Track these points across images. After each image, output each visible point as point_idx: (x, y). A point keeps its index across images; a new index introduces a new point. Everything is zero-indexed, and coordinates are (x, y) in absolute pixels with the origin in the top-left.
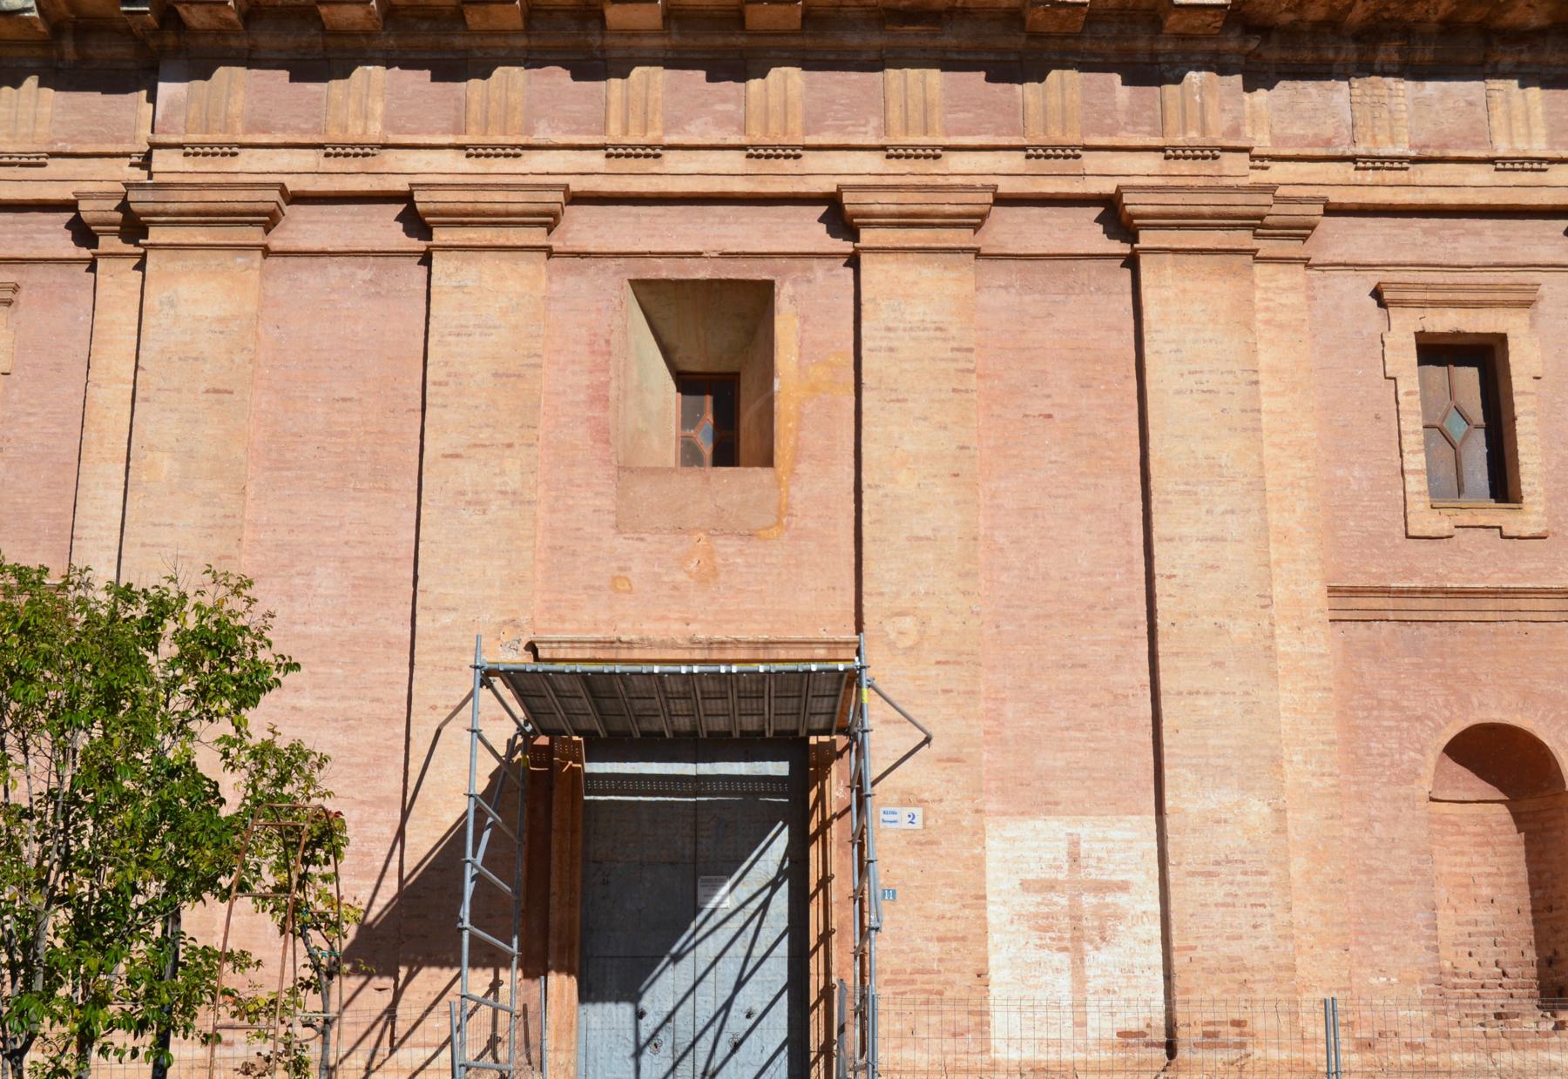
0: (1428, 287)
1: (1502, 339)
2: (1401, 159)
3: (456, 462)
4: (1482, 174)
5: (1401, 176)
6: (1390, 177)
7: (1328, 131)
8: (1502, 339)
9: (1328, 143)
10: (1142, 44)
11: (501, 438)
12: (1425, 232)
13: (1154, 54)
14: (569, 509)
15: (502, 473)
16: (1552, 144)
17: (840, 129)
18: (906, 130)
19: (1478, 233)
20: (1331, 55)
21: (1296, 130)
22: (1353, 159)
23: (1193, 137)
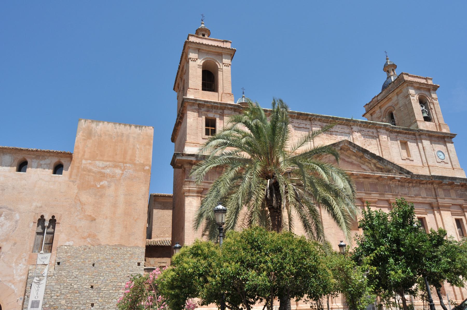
0: (418, 212)
1: (425, 218)
2: (413, 197)
3: (327, 229)
4: (421, 199)
5: (414, 198)
6: (412, 198)
7: (406, 193)
8: (425, 218)
9: (406, 194)
10: (389, 182)
11: (332, 227)
12: (416, 205)
13: (390, 183)
14: (339, 235)
15: (332, 231)
16: (427, 196)
17: (360, 190)
18: (367, 191)
19: (421, 205)
20: (405, 184)
21: (403, 193)
22: (409, 196)
23: (394, 193)
